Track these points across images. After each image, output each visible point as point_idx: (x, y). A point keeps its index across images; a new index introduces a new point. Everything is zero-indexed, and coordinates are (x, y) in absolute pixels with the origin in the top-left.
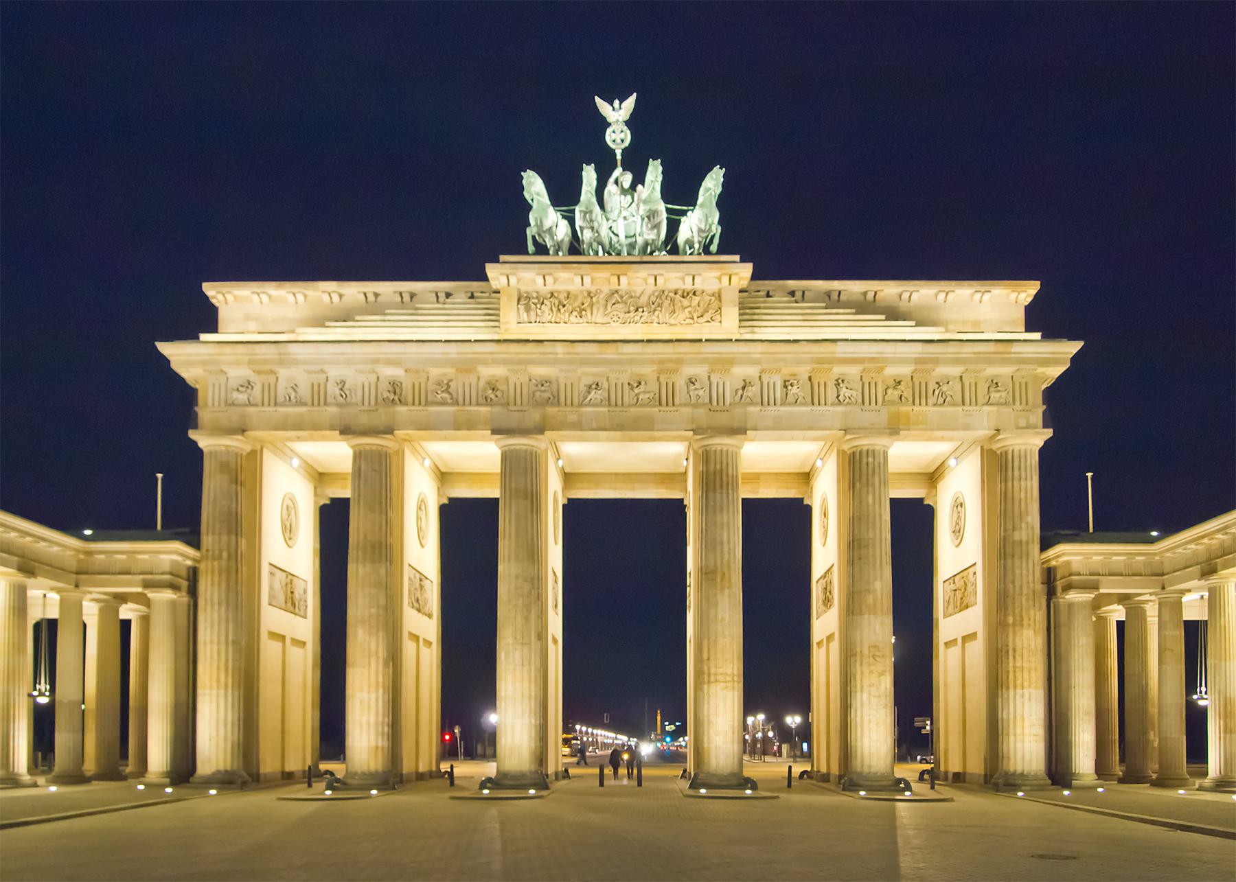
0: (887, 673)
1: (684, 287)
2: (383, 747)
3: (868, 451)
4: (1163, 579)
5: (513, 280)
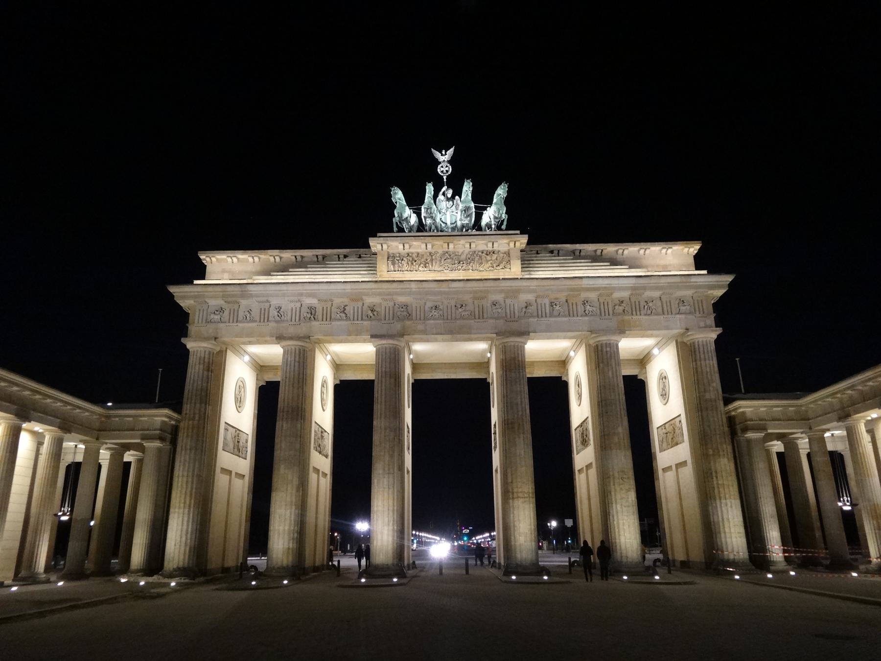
0: (632, 490)
1: (487, 249)
2: (293, 548)
3: (606, 344)
4: (810, 423)
5: (385, 246)
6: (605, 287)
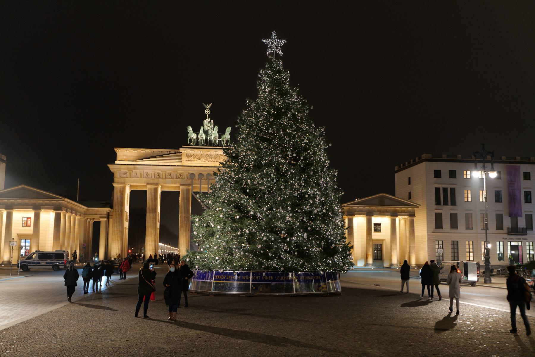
5: (185, 151)
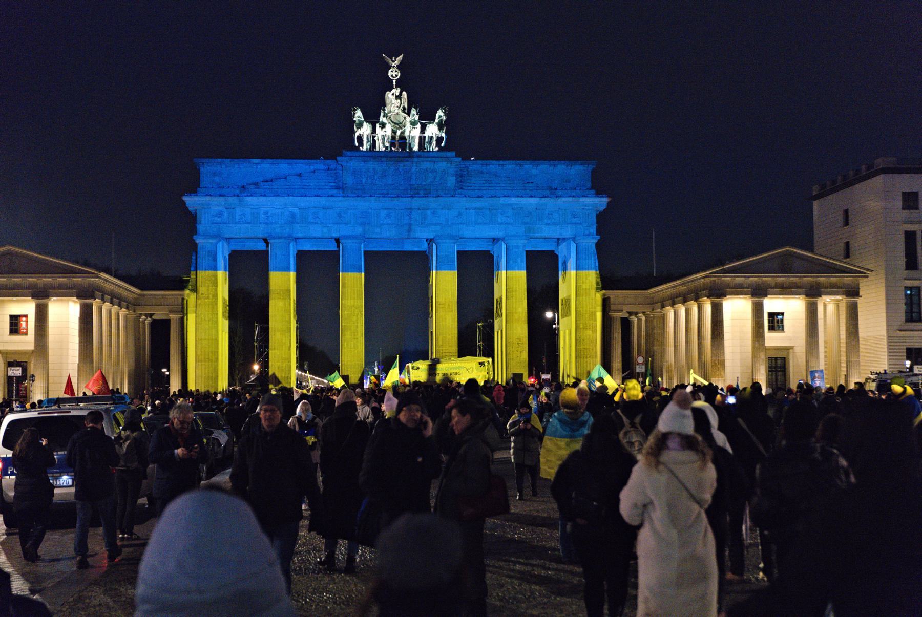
6: (517, 204)
